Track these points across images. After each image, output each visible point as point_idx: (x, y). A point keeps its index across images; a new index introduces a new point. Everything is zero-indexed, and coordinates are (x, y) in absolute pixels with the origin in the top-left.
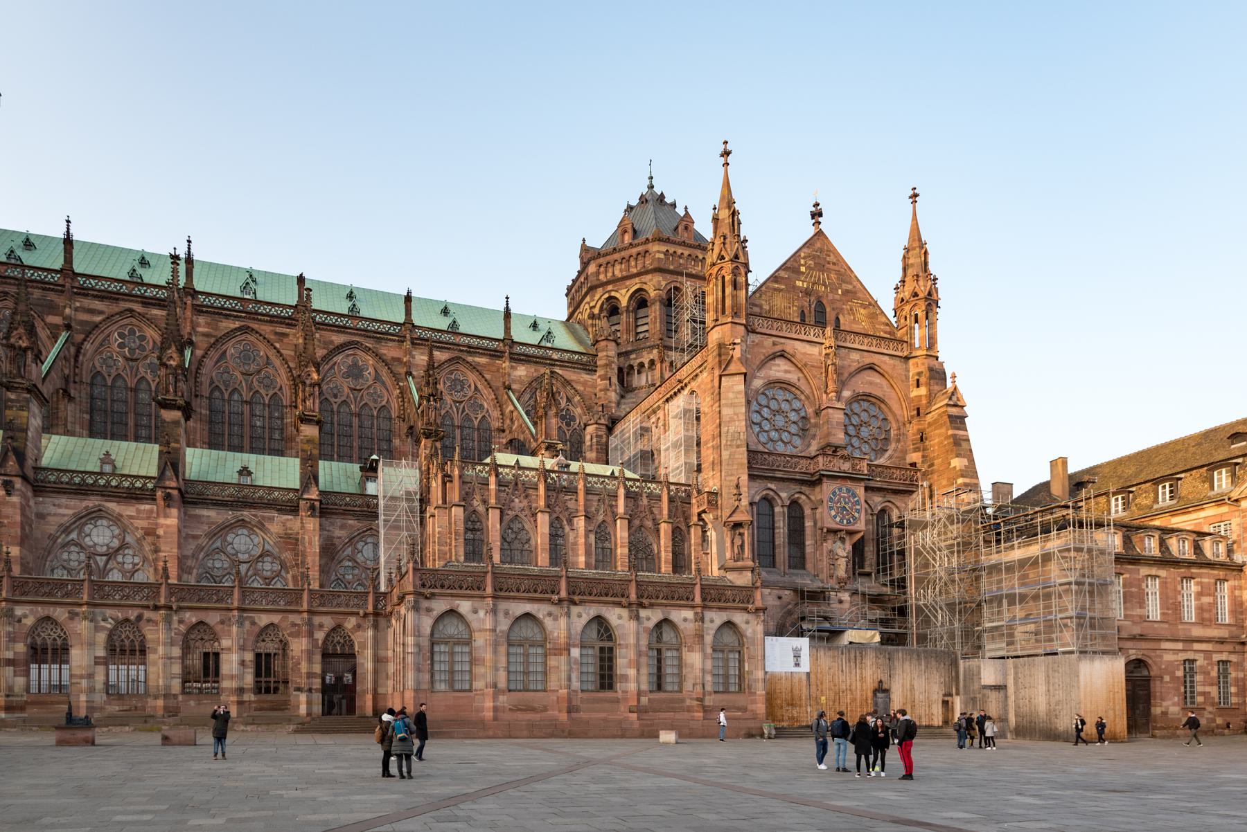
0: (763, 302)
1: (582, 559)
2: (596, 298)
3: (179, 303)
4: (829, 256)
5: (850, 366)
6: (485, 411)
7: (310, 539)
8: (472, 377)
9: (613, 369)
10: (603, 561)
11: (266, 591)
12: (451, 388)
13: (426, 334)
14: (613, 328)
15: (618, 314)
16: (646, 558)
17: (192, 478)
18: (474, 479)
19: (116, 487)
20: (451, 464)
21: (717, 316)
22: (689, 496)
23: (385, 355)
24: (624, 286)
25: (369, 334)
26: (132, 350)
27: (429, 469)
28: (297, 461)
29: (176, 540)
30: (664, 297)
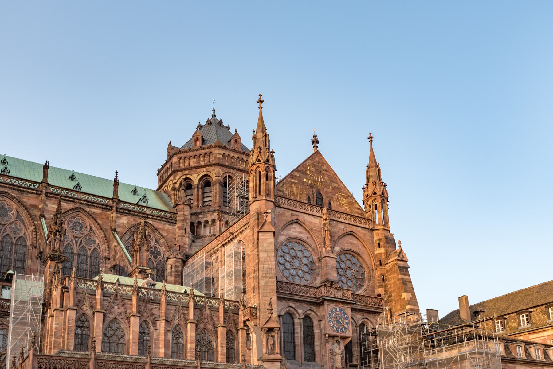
0: (285, 189)
1: (162, 351)
2: (178, 177)
4: (324, 166)
5: (338, 232)
6: (96, 245)
8: (88, 222)
9: (188, 223)
10: (177, 353)
12: (73, 228)
14: (188, 197)
15: (192, 189)
16: (208, 351)
18: (85, 291)
20: (69, 280)
21: (256, 195)
22: (238, 309)
24: (196, 172)
27: (52, 282)
30: (222, 181)
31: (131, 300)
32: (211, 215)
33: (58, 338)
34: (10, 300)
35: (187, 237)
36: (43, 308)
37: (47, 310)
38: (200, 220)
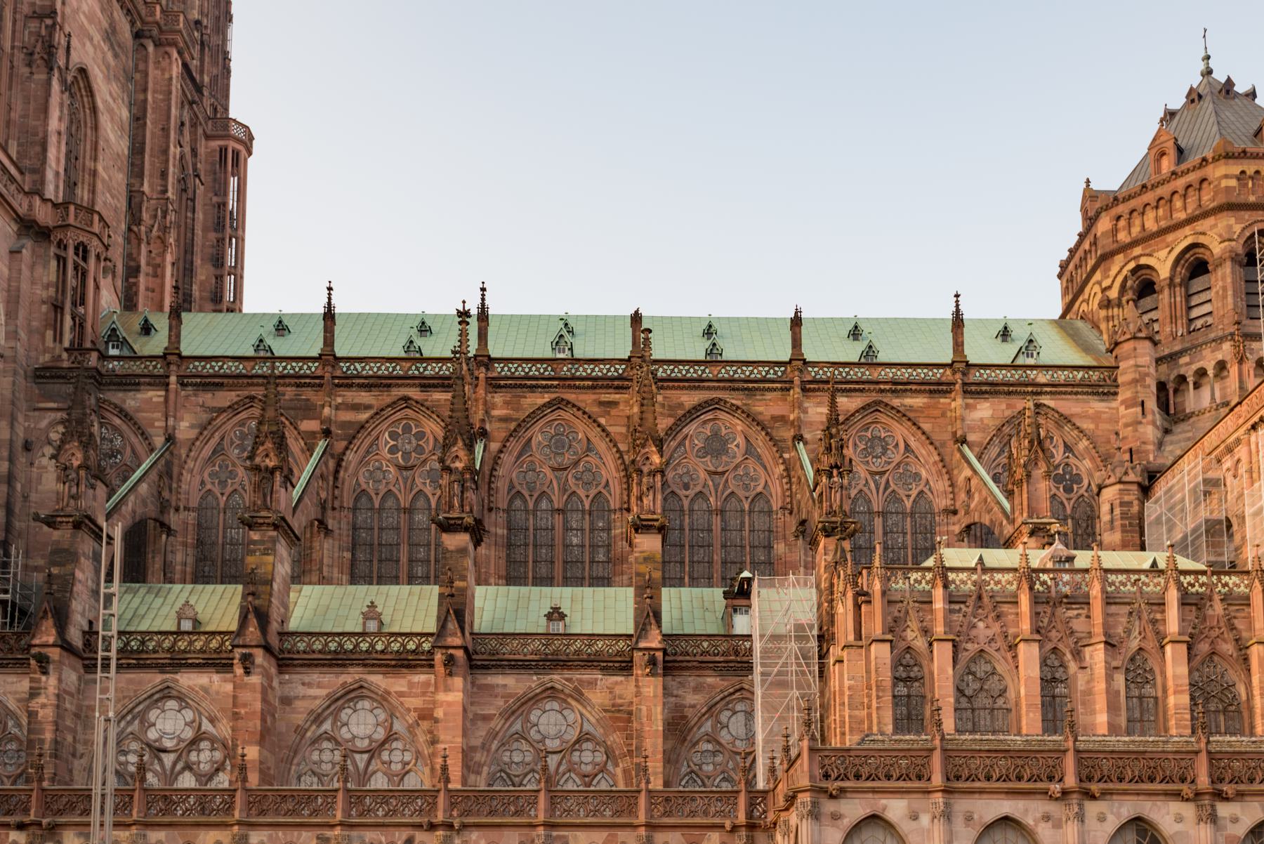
1: (1102, 718)
3: (468, 378)
7: (649, 710)
8: (900, 431)
9: (1149, 386)
10: (1141, 721)
11: (586, 795)
13: (825, 373)
14: (1146, 318)
15: (1154, 292)
17: (482, 631)
18: (908, 595)
19: (382, 652)
20: (869, 574)
23: (761, 413)
25: (736, 385)
26: (406, 455)
27: (832, 585)
28: (630, 591)
29: (460, 723)
30: (1240, 250)
31: (1017, 603)
32: (1213, 352)
33: (856, 708)
34: (751, 636)
35: (1148, 423)
36: (820, 646)
37: (828, 650)
38: (1182, 371)
